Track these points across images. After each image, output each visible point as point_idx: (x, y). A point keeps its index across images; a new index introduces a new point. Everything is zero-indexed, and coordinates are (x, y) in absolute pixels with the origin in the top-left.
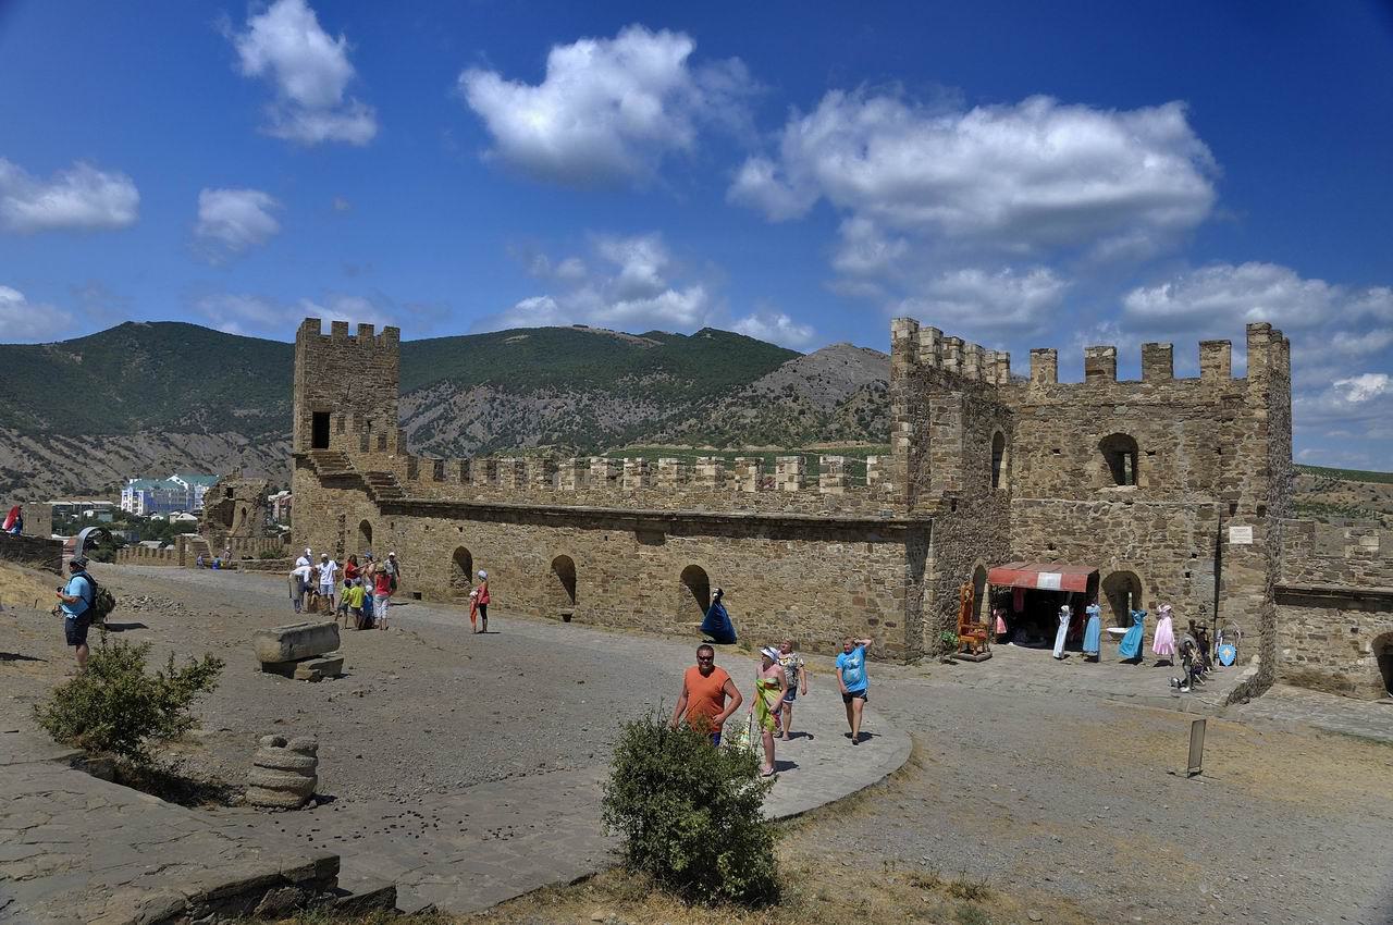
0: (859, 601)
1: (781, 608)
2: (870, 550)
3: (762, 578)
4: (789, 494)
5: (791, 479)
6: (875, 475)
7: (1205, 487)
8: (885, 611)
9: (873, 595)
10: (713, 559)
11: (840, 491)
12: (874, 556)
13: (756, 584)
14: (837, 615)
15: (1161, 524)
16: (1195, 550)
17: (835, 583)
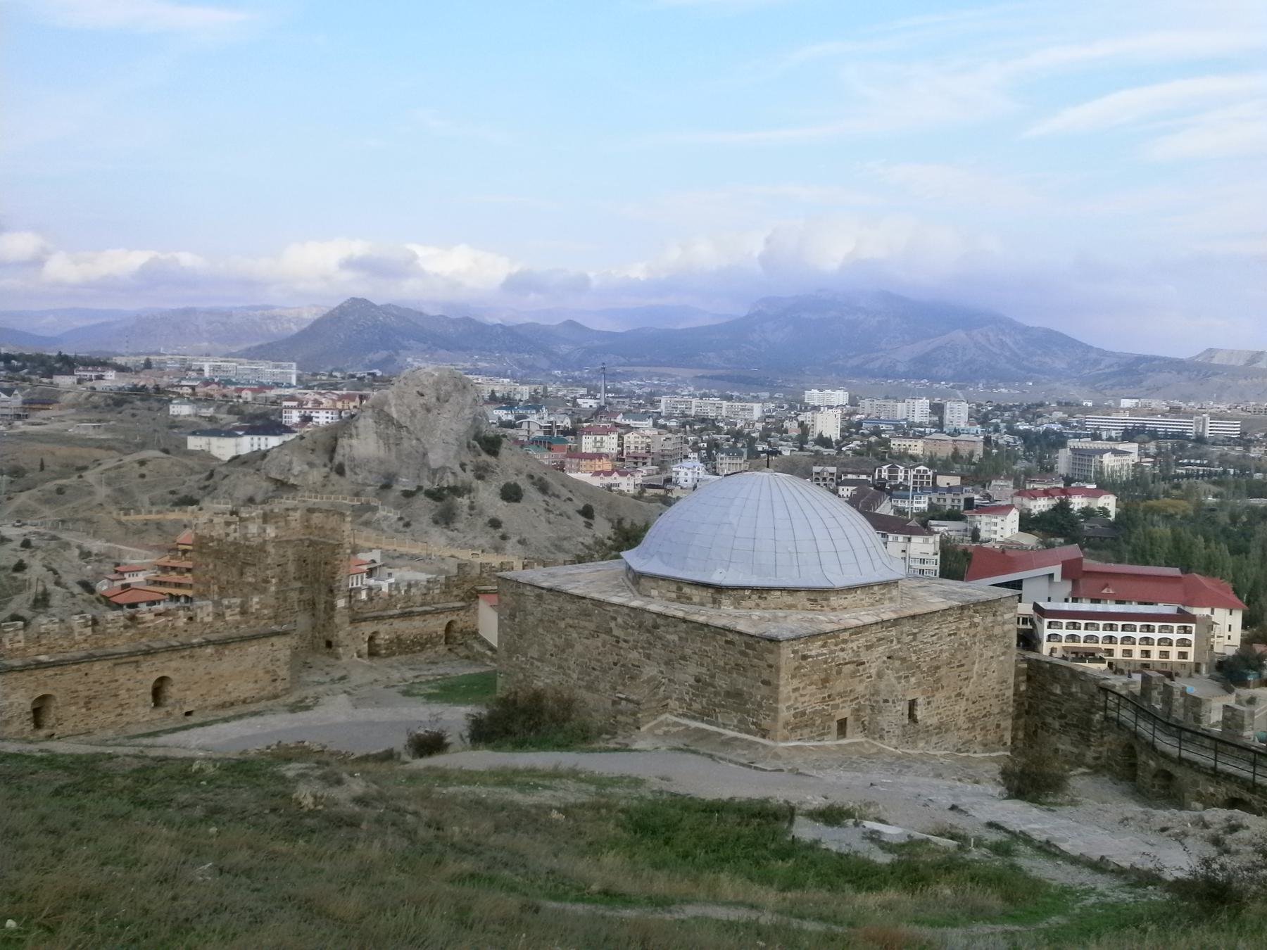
0: (268, 672)
1: (223, 686)
2: (272, 645)
3: (210, 673)
4: (207, 624)
5: (208, 615)
6: (258, 607)
7: (300, 578)
8: (280, 673)
9: (274, 667)
10: (177, 670)
11: (238, 618)
12: (275, 648)
13: (207, 677)
14: (256, 682)
15: (285, 600)
16: (297, 609)
17: (253, 666)
